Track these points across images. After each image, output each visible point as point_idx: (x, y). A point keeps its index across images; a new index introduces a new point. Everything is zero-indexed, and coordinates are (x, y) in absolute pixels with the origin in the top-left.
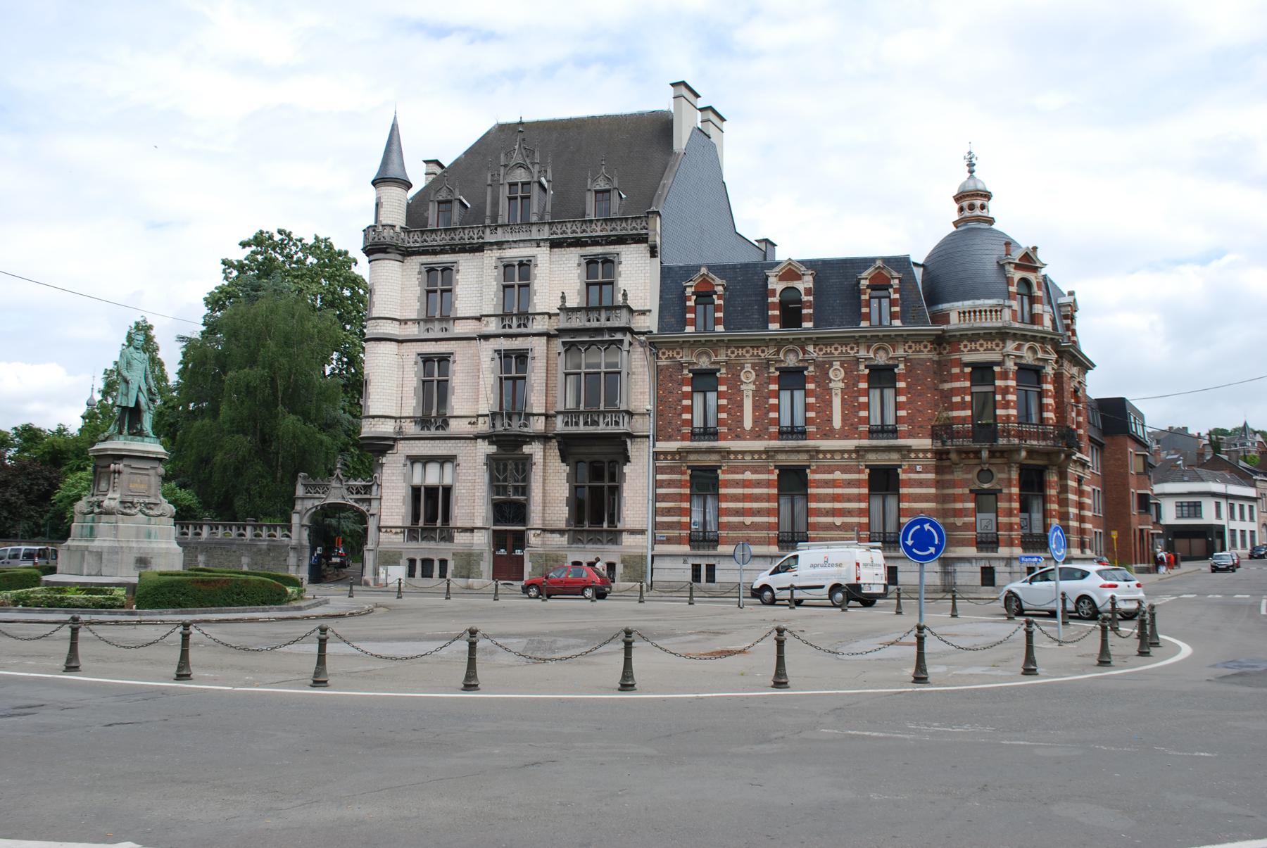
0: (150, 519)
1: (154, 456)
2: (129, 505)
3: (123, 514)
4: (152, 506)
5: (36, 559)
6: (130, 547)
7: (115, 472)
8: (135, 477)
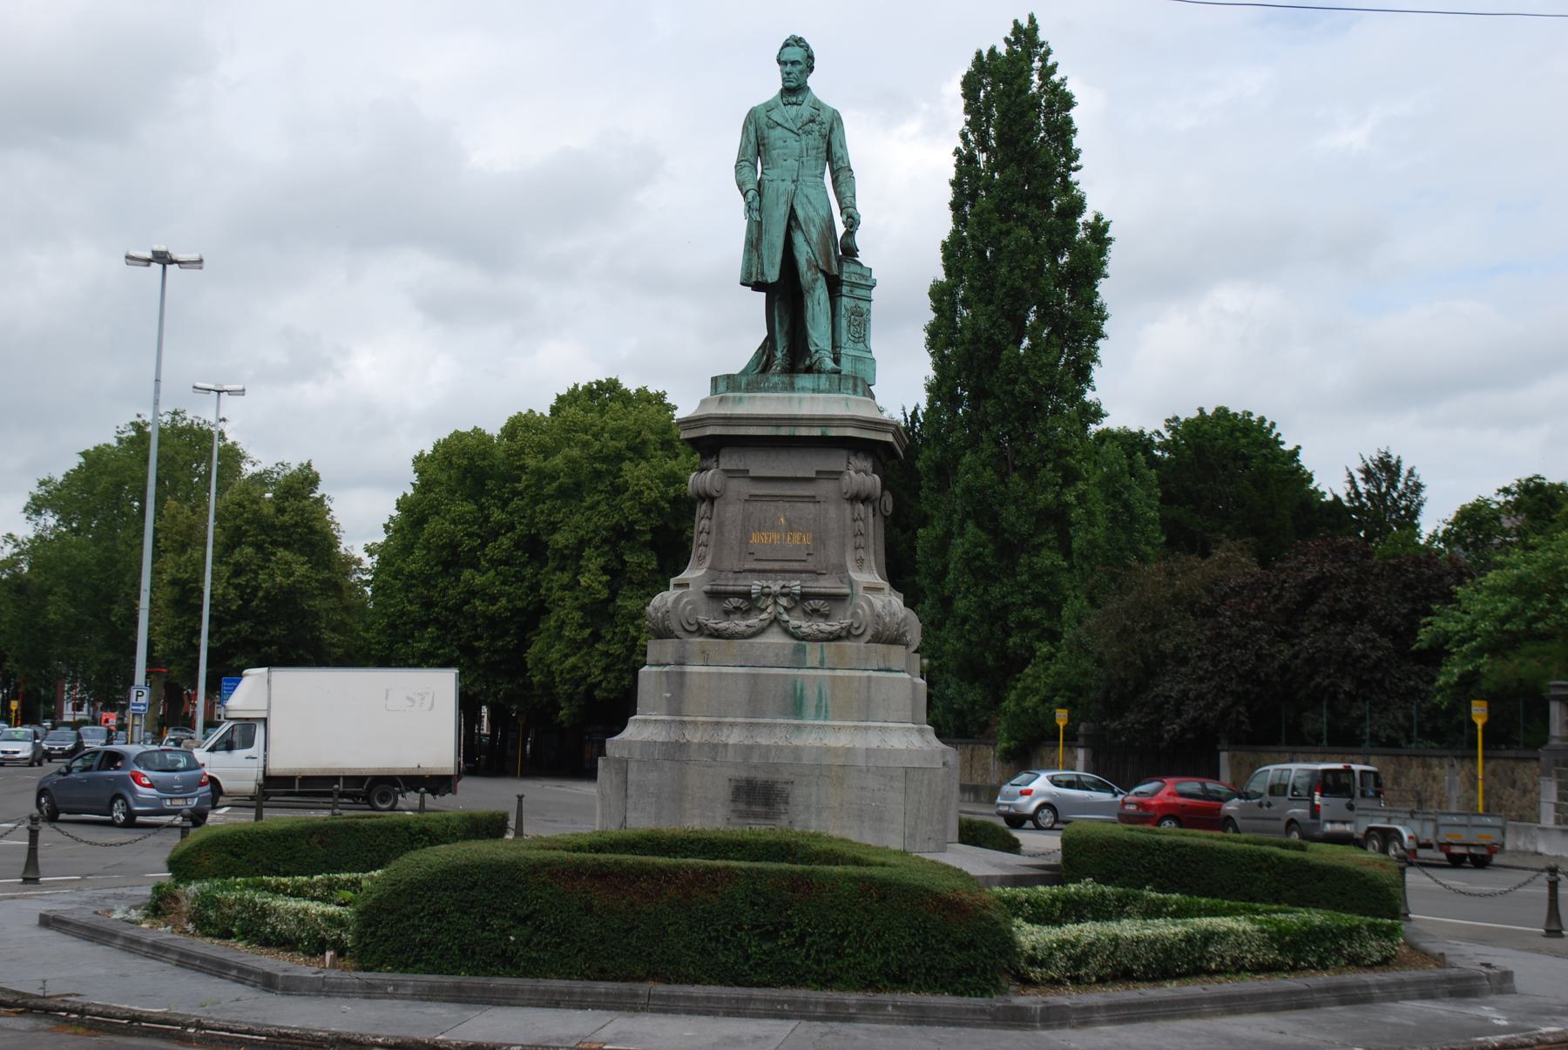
0: (799, 651)
1: (817, 432)
2: (735, 602)
5: (1317, 796)
6: (715, 746)
8: (770, 508)
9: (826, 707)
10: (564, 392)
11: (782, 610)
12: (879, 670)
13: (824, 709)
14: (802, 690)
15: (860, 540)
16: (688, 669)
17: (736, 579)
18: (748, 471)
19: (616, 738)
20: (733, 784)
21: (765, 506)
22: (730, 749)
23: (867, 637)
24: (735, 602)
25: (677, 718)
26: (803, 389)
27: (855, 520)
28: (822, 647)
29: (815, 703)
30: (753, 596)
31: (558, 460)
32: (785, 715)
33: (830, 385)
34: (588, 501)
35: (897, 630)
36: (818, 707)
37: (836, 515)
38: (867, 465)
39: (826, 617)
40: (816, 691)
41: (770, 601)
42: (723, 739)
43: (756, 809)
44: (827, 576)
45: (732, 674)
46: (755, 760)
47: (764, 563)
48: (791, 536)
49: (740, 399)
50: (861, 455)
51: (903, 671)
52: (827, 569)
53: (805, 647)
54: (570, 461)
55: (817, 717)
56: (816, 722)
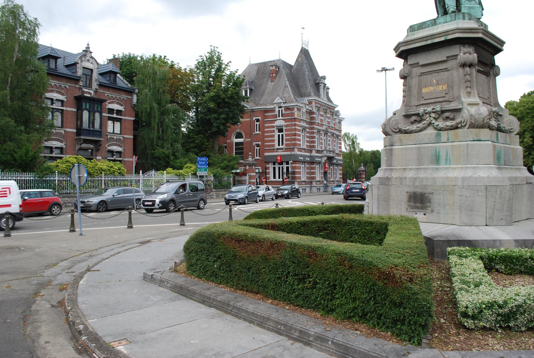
0: (438, 135)
1: (442, 39)
6: (401, 178)
9: (450, 159)
10: (522, 95)
11: (432, 119)
12: (474, 141)
13: (449, 160)
14: (439, 153)
15: (468, 84)
16: (394, 147)
17: (416, 109)
18: (418, 63)
19: (375, 176)
20: (409, 194)
21: (427, 76)
22: (407, 179)
23: (467, 126)
24: (414, 118)
25: (390, 168)
26: (440, 23)
27: (465, 75)
28: (448, 132)
30: (421, 114)
31: (518, 111)
32: (432, 164)
34: (526, 120)
35: (483, 121)
36: (446, 159)
37: (458, 74)
38: (471, 49)
39: (453, 119)
40: (445, 152)
41: (428, 116)
42: (406, 175)
43: (418, 205)
44: (454, 102)
45: (411, 148)
46: (417, 184)
47: (428, 100)
48: (438, 87)
49: (414, 34)
50: (467, 46)
51: (488, 141)
52: (454, 99)
54: (520, 111)
55: (446, 164)
56: (445, 166)
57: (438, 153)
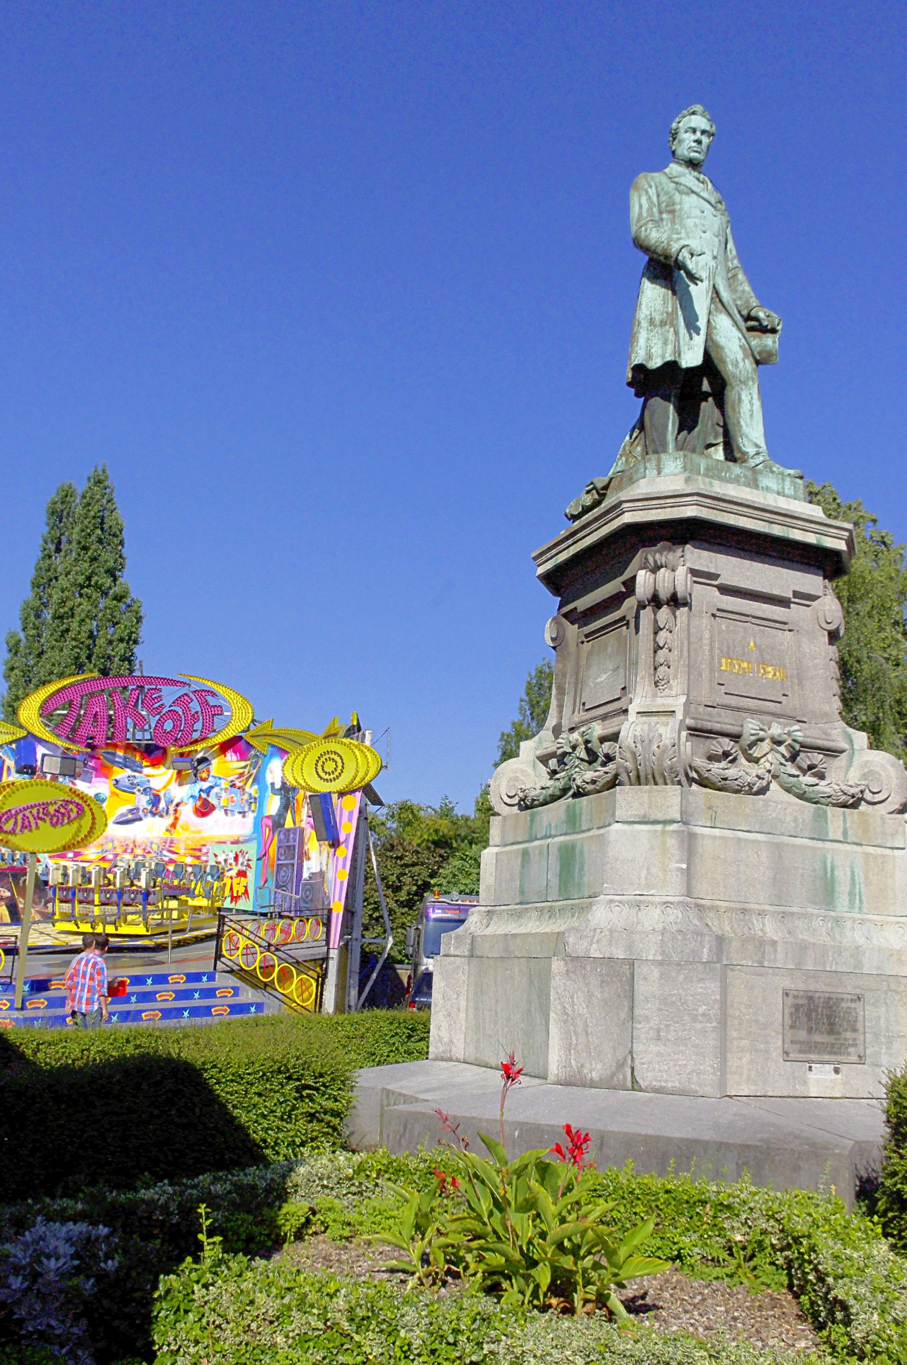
0: (820, 817)
2: (726, 744)
3: (703, 783)
4: (817, 758)
7: (656, 601)
9: (860, 892)
13: (858, 897)
14: (832, 871)
20: (790, 1001)
28: (844, 813)
29: (848, 889)
33: (795, 491)
40: (849, 873)
43: (817, 1038)
45: (754, 841)
53: (826, 812)
57: (829, 870)
